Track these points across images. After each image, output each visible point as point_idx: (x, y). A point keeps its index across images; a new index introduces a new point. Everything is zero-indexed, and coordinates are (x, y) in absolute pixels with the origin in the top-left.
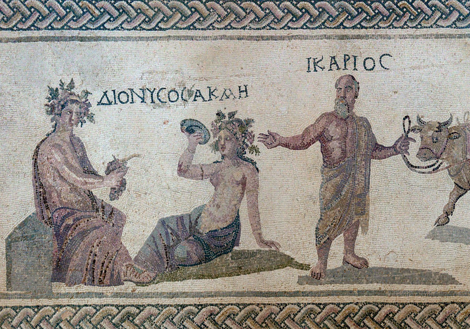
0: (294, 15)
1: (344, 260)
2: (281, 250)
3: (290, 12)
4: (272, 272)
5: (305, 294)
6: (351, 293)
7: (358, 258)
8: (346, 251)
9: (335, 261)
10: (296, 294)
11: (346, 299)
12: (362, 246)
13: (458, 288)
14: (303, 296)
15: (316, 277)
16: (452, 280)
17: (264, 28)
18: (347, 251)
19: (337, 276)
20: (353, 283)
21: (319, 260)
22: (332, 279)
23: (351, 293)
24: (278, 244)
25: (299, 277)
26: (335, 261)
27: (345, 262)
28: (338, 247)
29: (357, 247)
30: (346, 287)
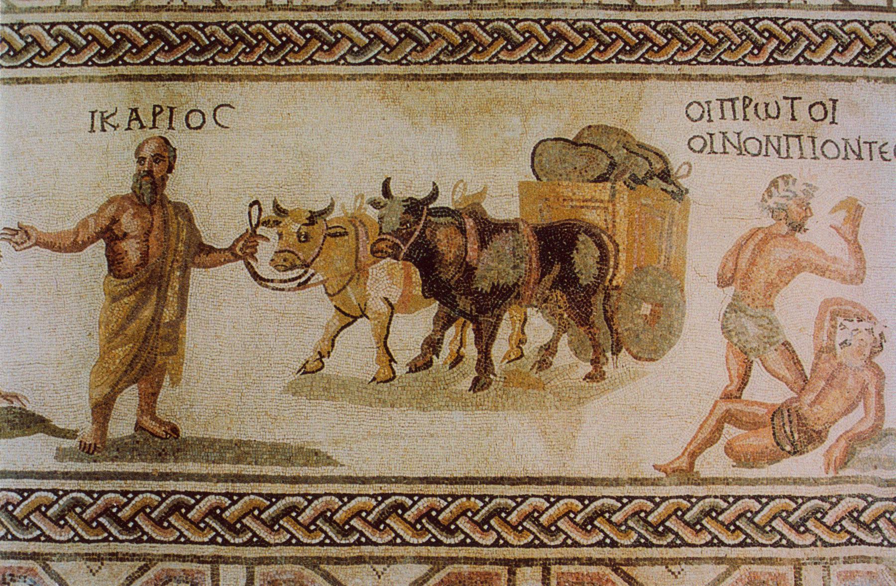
0: (73, 46)
1: (136, 425)
2: (29, 408)
3: (67, 40)
4: (13, 440)
5: (66, 476)
6: (146, 476)
7: (161, 423)
8: (142, 411)
9: (122, 425)
10: (52, 475)
11: (138, 485)
12: (168, 402)
13: (337, 472)
14: (63, 478)
15: (88, 451)
16: (329, 461)
17: (22, 65)
18: (142, 411)
19: (123, 449)
20: (152, 461)
21: (93, 424)
22: (115, 453)
23: (146, 476)
24: (25, 398)
25: (57, 449)
26: (122, 425)
27: (139, 427)
28: (128, 403)
29: (159, 405)
30: (137, 467)
